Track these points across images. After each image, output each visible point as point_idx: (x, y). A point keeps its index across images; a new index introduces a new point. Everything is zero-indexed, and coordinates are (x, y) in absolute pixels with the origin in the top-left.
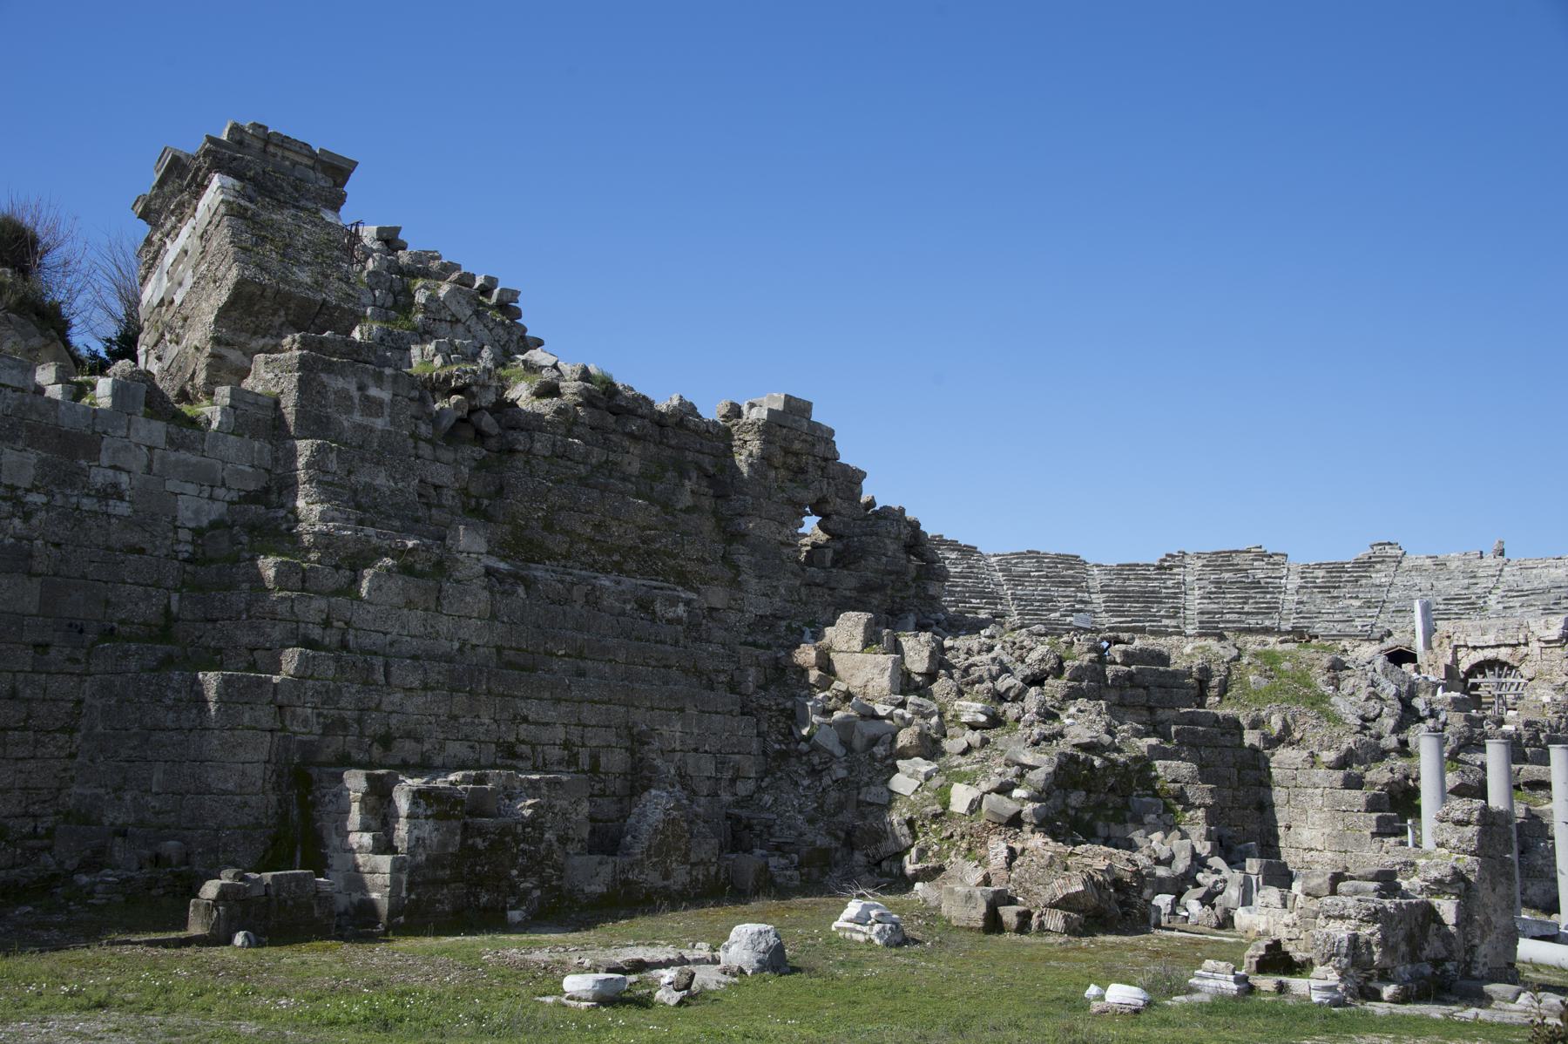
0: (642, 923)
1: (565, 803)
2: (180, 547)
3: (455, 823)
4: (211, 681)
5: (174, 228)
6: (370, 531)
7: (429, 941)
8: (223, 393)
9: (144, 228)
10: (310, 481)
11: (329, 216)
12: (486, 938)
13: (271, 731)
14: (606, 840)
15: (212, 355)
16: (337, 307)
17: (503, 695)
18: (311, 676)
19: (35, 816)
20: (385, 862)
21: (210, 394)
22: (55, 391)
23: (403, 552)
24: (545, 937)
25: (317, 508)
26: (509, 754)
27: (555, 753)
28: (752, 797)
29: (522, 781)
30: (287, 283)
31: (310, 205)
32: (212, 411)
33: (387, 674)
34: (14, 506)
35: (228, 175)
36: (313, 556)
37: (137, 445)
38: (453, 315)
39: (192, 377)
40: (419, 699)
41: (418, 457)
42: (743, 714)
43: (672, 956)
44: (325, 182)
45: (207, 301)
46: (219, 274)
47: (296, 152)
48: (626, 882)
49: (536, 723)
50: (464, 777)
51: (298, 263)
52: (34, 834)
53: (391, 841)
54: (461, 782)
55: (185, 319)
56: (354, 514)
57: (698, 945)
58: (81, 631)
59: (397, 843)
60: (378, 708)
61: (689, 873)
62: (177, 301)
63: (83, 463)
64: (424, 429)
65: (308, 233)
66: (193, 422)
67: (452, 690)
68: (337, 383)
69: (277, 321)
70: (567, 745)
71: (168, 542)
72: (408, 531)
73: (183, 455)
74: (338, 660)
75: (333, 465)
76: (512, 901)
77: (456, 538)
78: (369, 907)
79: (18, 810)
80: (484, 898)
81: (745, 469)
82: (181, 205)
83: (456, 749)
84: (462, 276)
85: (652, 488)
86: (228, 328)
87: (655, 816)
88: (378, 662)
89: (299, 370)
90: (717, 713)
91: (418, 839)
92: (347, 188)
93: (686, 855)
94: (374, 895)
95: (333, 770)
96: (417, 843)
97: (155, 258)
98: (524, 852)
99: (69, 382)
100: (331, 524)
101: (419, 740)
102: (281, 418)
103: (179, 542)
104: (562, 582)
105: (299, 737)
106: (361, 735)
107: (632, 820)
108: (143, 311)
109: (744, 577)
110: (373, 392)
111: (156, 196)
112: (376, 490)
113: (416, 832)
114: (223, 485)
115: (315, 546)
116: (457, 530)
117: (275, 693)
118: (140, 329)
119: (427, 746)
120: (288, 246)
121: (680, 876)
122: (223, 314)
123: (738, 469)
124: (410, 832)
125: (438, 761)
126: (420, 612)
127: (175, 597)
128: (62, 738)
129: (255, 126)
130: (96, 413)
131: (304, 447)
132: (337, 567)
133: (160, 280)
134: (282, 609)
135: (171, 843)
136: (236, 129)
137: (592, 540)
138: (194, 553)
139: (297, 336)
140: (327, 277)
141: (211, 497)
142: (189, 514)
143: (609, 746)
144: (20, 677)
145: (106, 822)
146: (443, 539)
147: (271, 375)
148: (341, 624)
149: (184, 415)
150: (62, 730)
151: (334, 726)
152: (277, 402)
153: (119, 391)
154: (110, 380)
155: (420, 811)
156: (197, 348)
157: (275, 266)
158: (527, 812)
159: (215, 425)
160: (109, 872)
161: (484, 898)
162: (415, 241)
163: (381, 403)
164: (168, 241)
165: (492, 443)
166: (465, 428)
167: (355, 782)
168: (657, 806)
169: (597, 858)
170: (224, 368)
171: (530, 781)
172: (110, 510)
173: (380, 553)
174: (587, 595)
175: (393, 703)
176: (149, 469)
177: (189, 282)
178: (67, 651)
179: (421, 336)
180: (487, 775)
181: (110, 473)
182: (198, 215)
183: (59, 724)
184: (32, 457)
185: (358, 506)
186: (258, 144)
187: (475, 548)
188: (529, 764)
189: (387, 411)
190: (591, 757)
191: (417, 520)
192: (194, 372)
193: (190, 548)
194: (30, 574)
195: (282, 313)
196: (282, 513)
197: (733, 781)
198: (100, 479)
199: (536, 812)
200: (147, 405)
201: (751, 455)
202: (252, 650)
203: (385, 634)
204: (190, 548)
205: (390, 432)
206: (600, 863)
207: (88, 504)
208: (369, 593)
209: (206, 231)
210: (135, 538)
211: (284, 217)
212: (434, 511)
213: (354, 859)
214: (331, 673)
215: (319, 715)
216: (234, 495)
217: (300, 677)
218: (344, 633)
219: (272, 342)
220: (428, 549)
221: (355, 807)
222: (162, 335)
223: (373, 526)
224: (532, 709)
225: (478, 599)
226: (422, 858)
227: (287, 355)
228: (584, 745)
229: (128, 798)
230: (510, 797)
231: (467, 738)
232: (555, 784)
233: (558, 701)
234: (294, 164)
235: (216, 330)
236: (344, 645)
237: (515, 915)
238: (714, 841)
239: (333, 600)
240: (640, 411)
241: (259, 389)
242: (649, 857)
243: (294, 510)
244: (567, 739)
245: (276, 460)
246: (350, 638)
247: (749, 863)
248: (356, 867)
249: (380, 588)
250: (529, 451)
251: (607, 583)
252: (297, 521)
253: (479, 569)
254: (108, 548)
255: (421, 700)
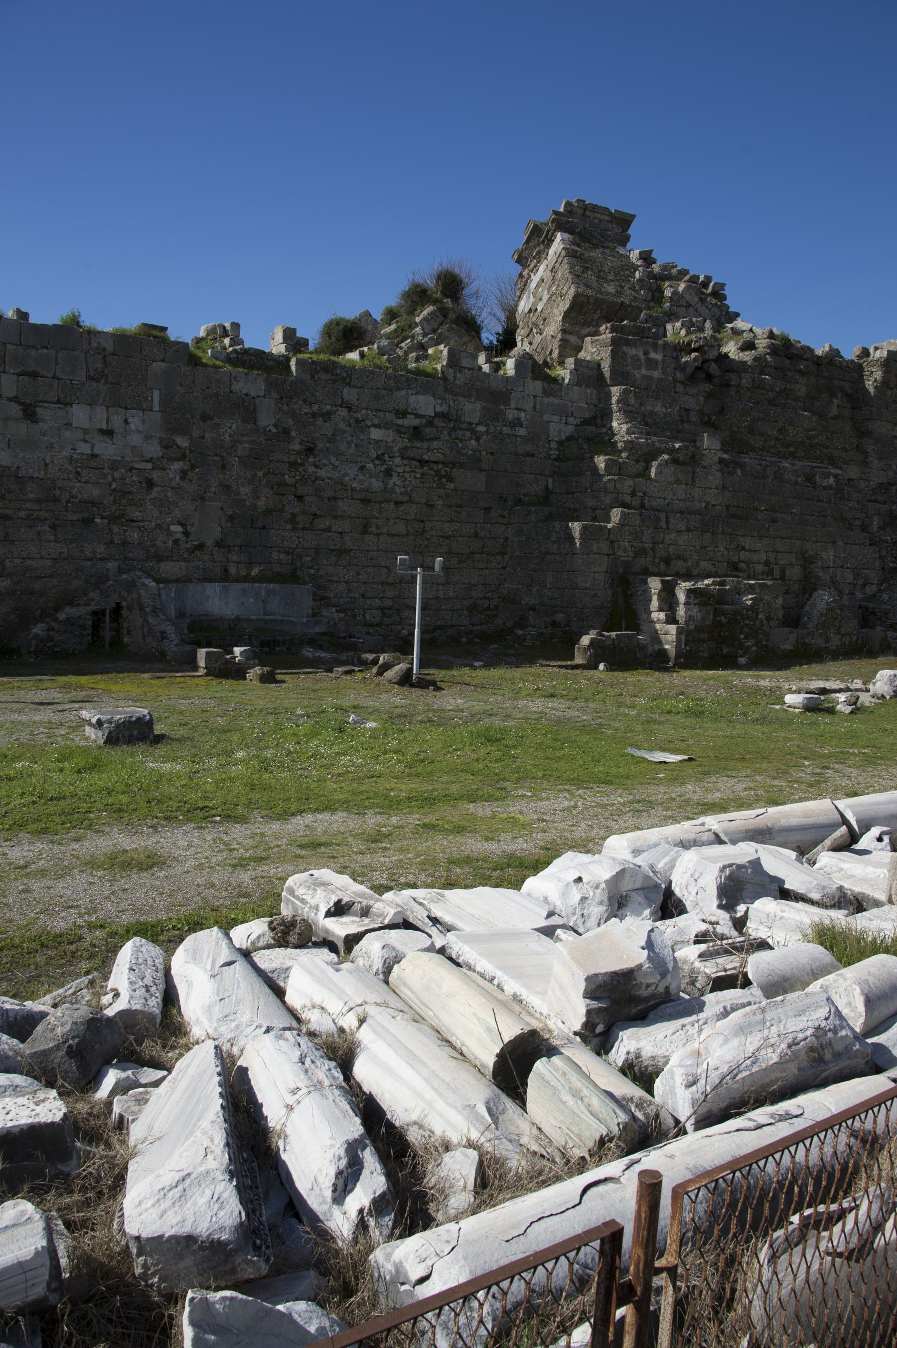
0: (816, 668)
1: (769, 598)
2: (552, 452)
3: (710, 608)
4: (576, 527)
5: (535, 266)
6: (654, 439)
7: (698, 672)
8: (570, 362)
9: (519, 268)
10: (620, 411)
11: (621, 251)
12: (730, 672)
13: (608, 555)
14: (793, 620)
15: (561, 340)
16: (630, 305)
17: (731, 534)
18: (627, 524)
19: (489, 599)
20: (673, 629)
21: (562, 363)
22: (486, 368)
23: (673, 451)
24: (763, 673)
25: (625, 427)
26: (735, 568)
27: (760, 568)
28: (875, 595)
29: (745, 584)
30: (601, 293)
31: (610, 245)
32: (564, 373)
33: (667, 523)
34: (472, 433)
35: (565, 232)
36: (624, 455)
37: (528, 395)
38: (687, 302)
39: (551, 353)
40: (685, 537)
41: (675, 392)
42: (871, 545)
43: (842, 687)
44: (618, 230)
45: (557, 308)
46: (563, 292)
47: (601, 214)
48: (804, 644)
49: (750, 551)
50: (713, 582)
51: (608, 281)
52: (489, 608)
53: (674, 617)
54: (712, 585)
55: (545, 320)
56: (645, 429)
57: (855, 681)
58: (505, 501)
59: (678, 618)
60: (663, 542)
61: (840, 640)
62: (539, 309)
63: (502, 407)
64: (679, 375)
65: (611, 262)
66: (555, 380)
67: (703, 531)
68: (632, 351)
69: (596, 317)
70: (767, 563)
71: (546, 450)
72: (677, 439)
73: (551, 399)
74: (641, 514)
75: (632, 401)
76: (741, 652)
77: (702, 441)
78: (663, 653)
79: (481, 595)
80: (725, 651)
81: (872, 390)
82: (539, 253)
83: (705, 565)
84: (691, 277)
85: (813, 405)
86: (569, 323)
87: (821, 606)
88: (662, 515)
89: (611, 345)
90: (855, 544)
91: (690, 616)
92: (629, 232)
93: (839, 629)
94: (667, 647)
95: (641, 577)
96: (689, 619)
97: (525, 285)
98: (747, 625)
99: (492, 362)
100: (633, 436)
101: (685, 560)
102: (601, 374)
103: (551, 449)
104: (760, 465)
105: (622, 559)
106: (654, 557)
107: (807, 608)
108: (519, 315)
109: (870, 459)
110: (652, 355)
111: (526, 249)
112: (655, 414)
113: (689, 613)
114: (572, 415)
115: (625, 449)
116: (703, 436)
117: (609, 534)
118: (518, 327)
119: (689, 564)
120: (600, 271)
121: (835, 641)
122: (567, 315)
123: (867, 390)
124: (686, 612)
125: (695, 572)
126: (683, 486)
127: (550, 480)
128: (499, 558)
129: (578, 201)
130: (507, 379)
131: (616, 391)
132: (637, 461)
133: (528, 297)
134: (610, 486)
135: (560, 615)
136: (568, 204)
137: (777, 439)
138: (559, 455)
139: (609, 325)
140: (622, 287)
141: (566, 423)
142: (556, 433)
143: (791, 564)
144: (479, 525)
145: (524, 602)
146: (694, 441)
147: (595, 349)
148: (641, 494)
149: (550, 376)
150: (499, 554)
151: (640, 552)
152: (599, 365)
153: (518, 366)
154: (514, 360)
155: (691, 601)
156: (552, 336)
157: (595, 284)
158: (749, 603)
159: (567, 381)
160: (530, 628)
161: (725, 651)
162: (661, 259)
163: (656, 362)
164: (532, 275)
165: (716, 381)
166: (700, 373)
167: (655, 584)
168: (823, 598)
169: (788, 630)
170: (569, 347)
171: (750, 585)
172: (517, 433)
173: (660, 452)
174: (775, 473)
175: (670, 539)
176: (535, 407)
177: (545, 298)
178: (499, 511)
179: (669, 316)
180: (725, 581)
181: (516, 412)
182: (549, 258)
183: (497, 551)
184: (478, 406)
185: (646, 424)
186: (580, 212)
187: (714, 447)
188: (745, 574)
189: (660, 366)
190: (781, 571)
191: (679, 431)
192: (551, 350)
193: (557, 452)
194: (481, 470)
195: (599, 312)
196: (604, 430)
197: (864, 585)
198: (511, 416)
199: (754, 602)
200: (532, 372)
201: (875, 381)
202: (594, 510)
203: (665, 499)
204: (557, 452)
205: (662, 379)
206: (790, 633)
207: (506, 430)
208: (655, 475)
209: (554, 267)
210: (529, 448)
211: (596, 254)
212: (685, 425)
213: (654, 627)
214: (637, 522)
215: (632, 546)
216: (578, 421)
217: (622, 524)
218: (643, 499)
219: (594, 330)
220: (686, 448)
221: (655, 598)
222: (532, 330)
223: (655, 435)
224: (747, 542)
225: (715, 478)
226: (692, 627)
227: (604, 336)
228: (777, 564)
229: (534, 590)
230: (739, 594)
231: (711, 559)
232: (763, 586)
233: (761, 537)
234: (600, 221)
235: (563, 325)
236: (642, 506)
237: (742, 661)
238: (856, 621)
239: (636, 480)
240: (805, 356)
241: (588, 358)
242: (818, 630)
243: (611, 428)
244: (767, 560)
245: (599, 399)
246: (646, 502)
247: (877, 633)
248: (656, 631)
249: (661, 472)
250: (739, 385)
251: (787, 465)
252: (614, 435)
253: (716, 459)
254: (517, 454)
255: (686, 538)
